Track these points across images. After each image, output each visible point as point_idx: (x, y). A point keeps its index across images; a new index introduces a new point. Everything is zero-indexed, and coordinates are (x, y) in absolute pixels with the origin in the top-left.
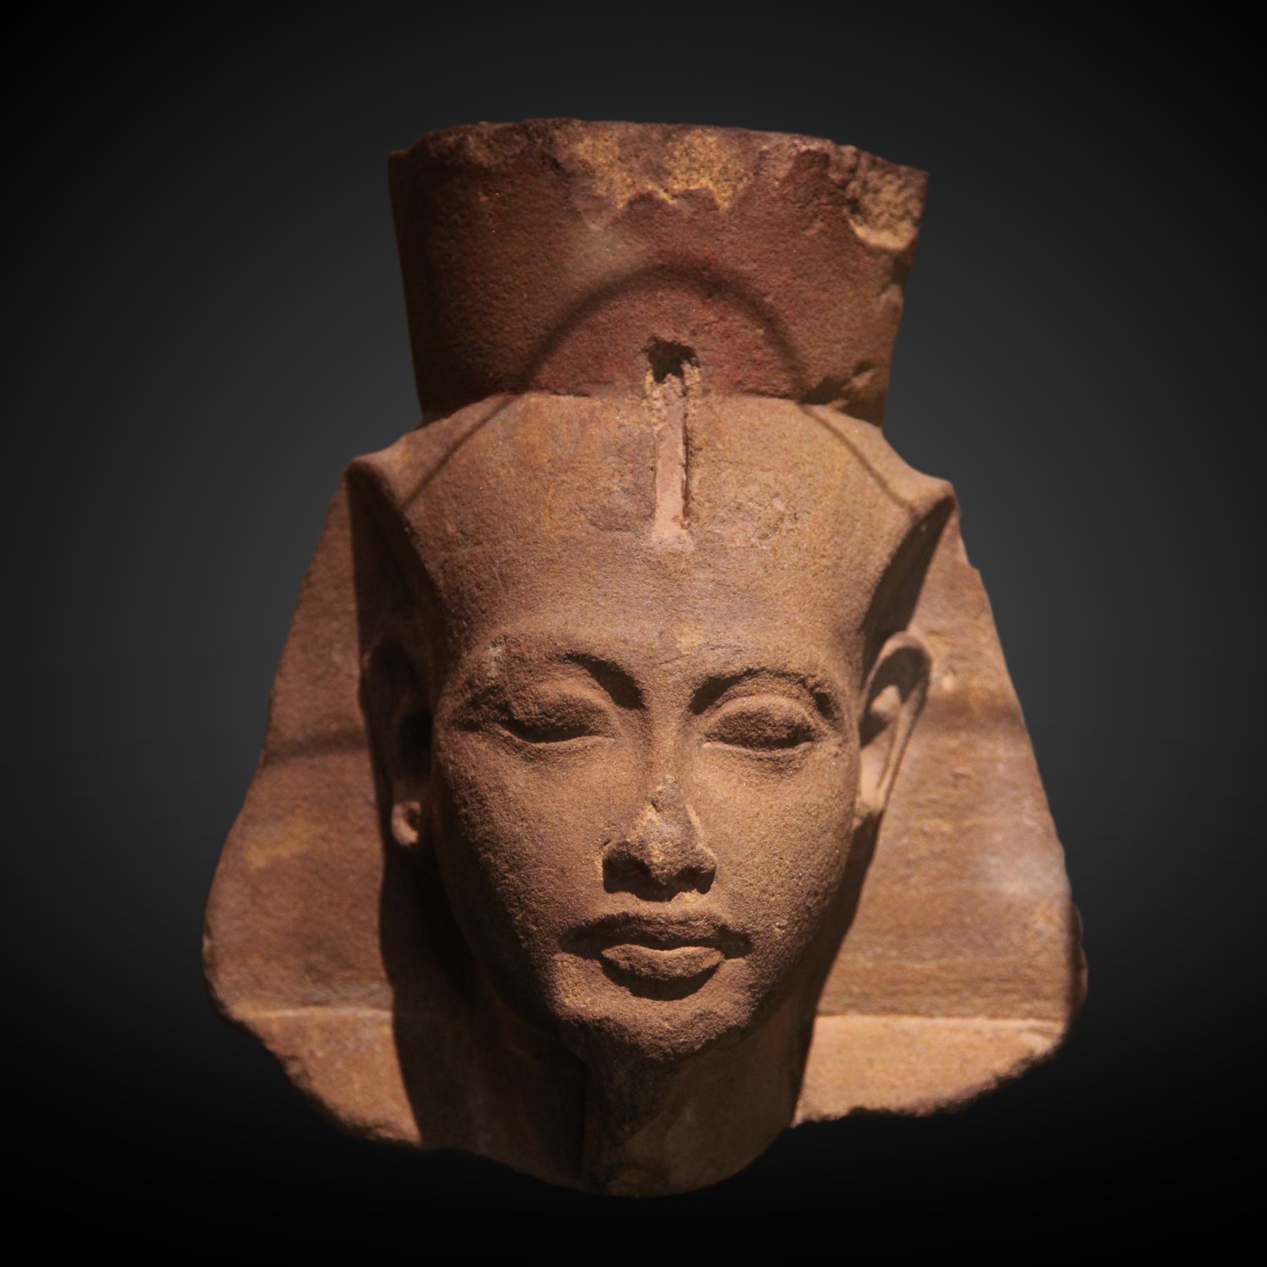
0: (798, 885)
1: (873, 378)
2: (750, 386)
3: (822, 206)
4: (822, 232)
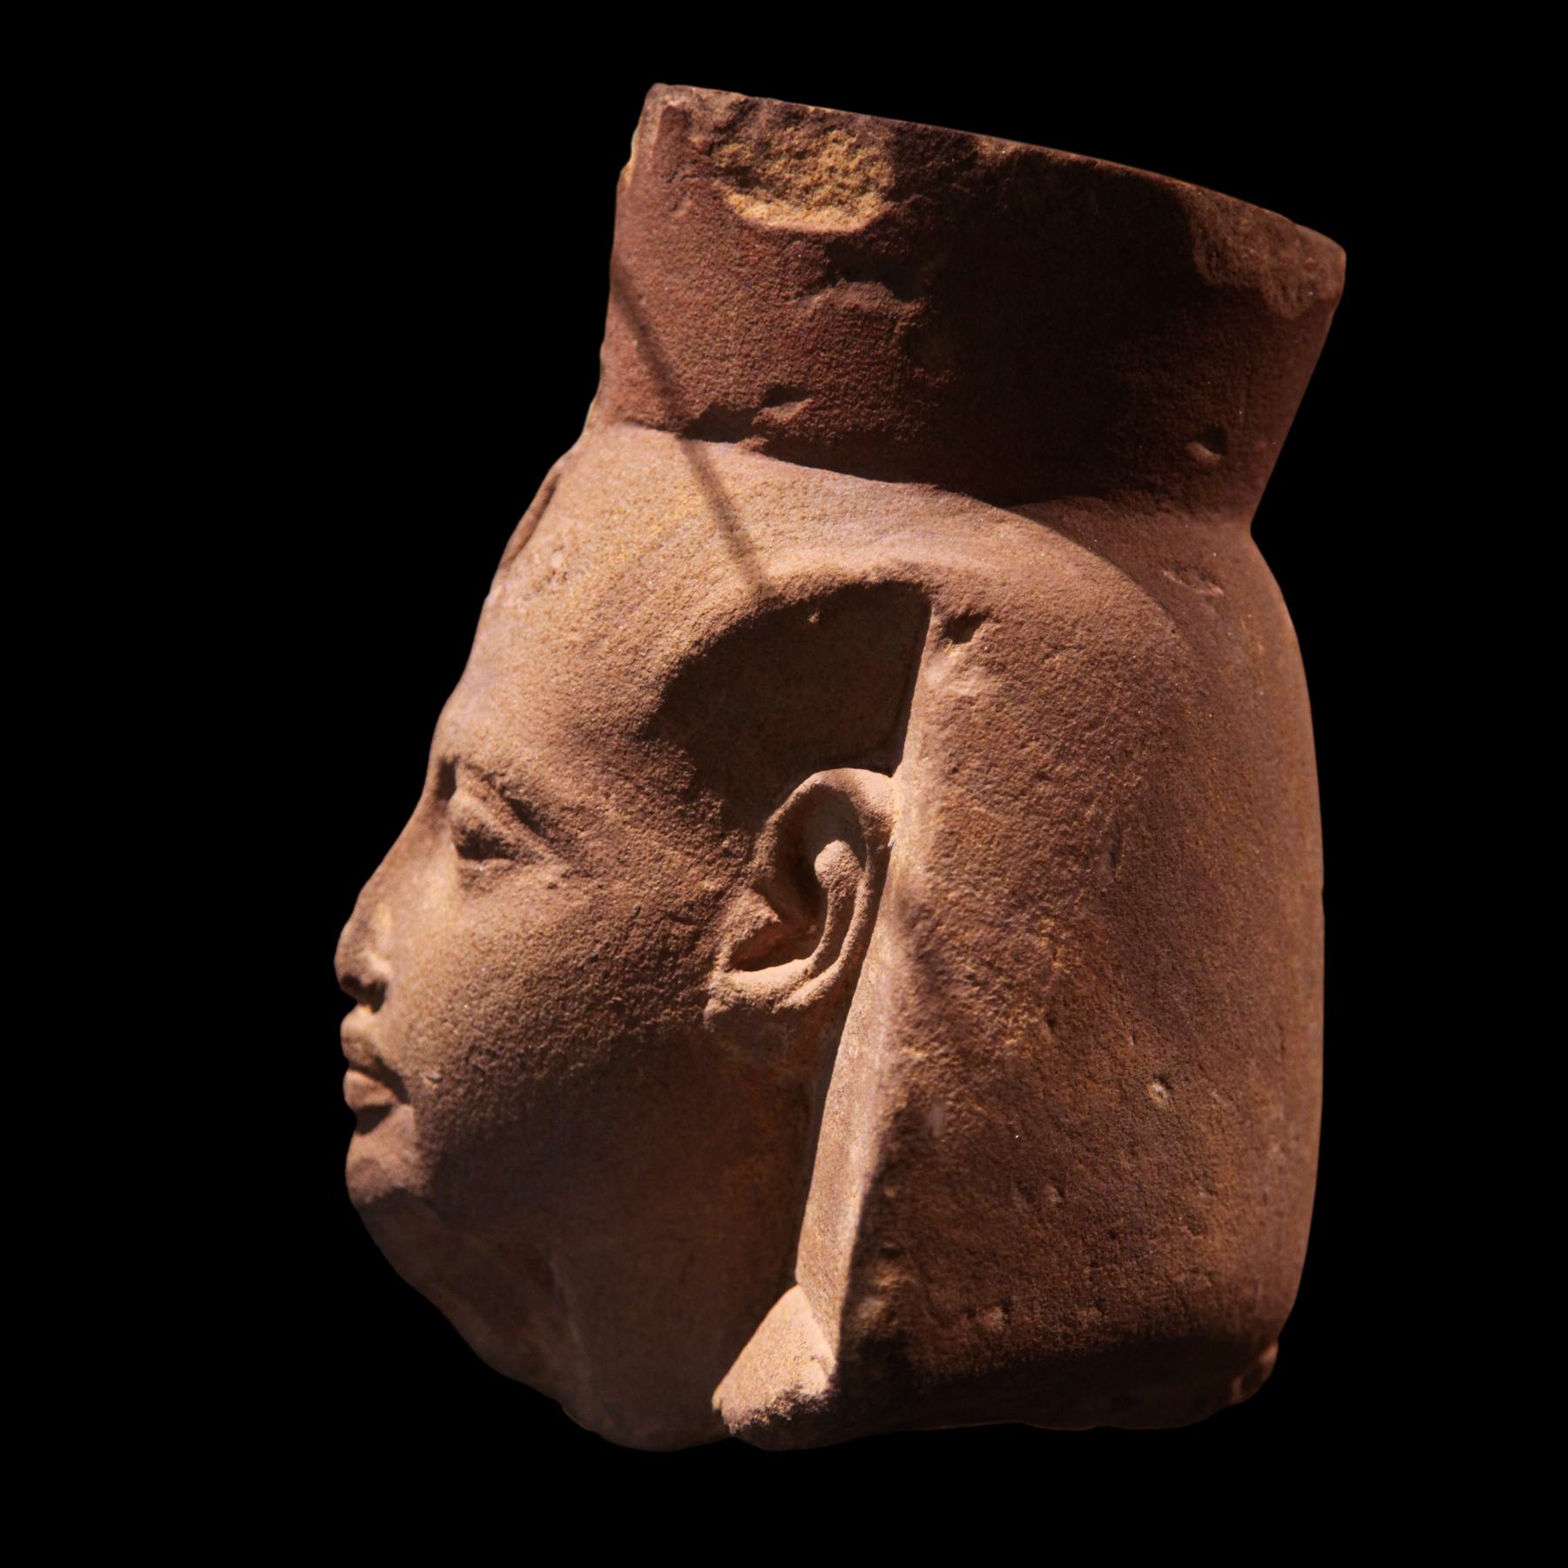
0: (451, 1032)
1: (811, 410)
2: (629, 413)
3: (688, 179)
4: (692, 212)
